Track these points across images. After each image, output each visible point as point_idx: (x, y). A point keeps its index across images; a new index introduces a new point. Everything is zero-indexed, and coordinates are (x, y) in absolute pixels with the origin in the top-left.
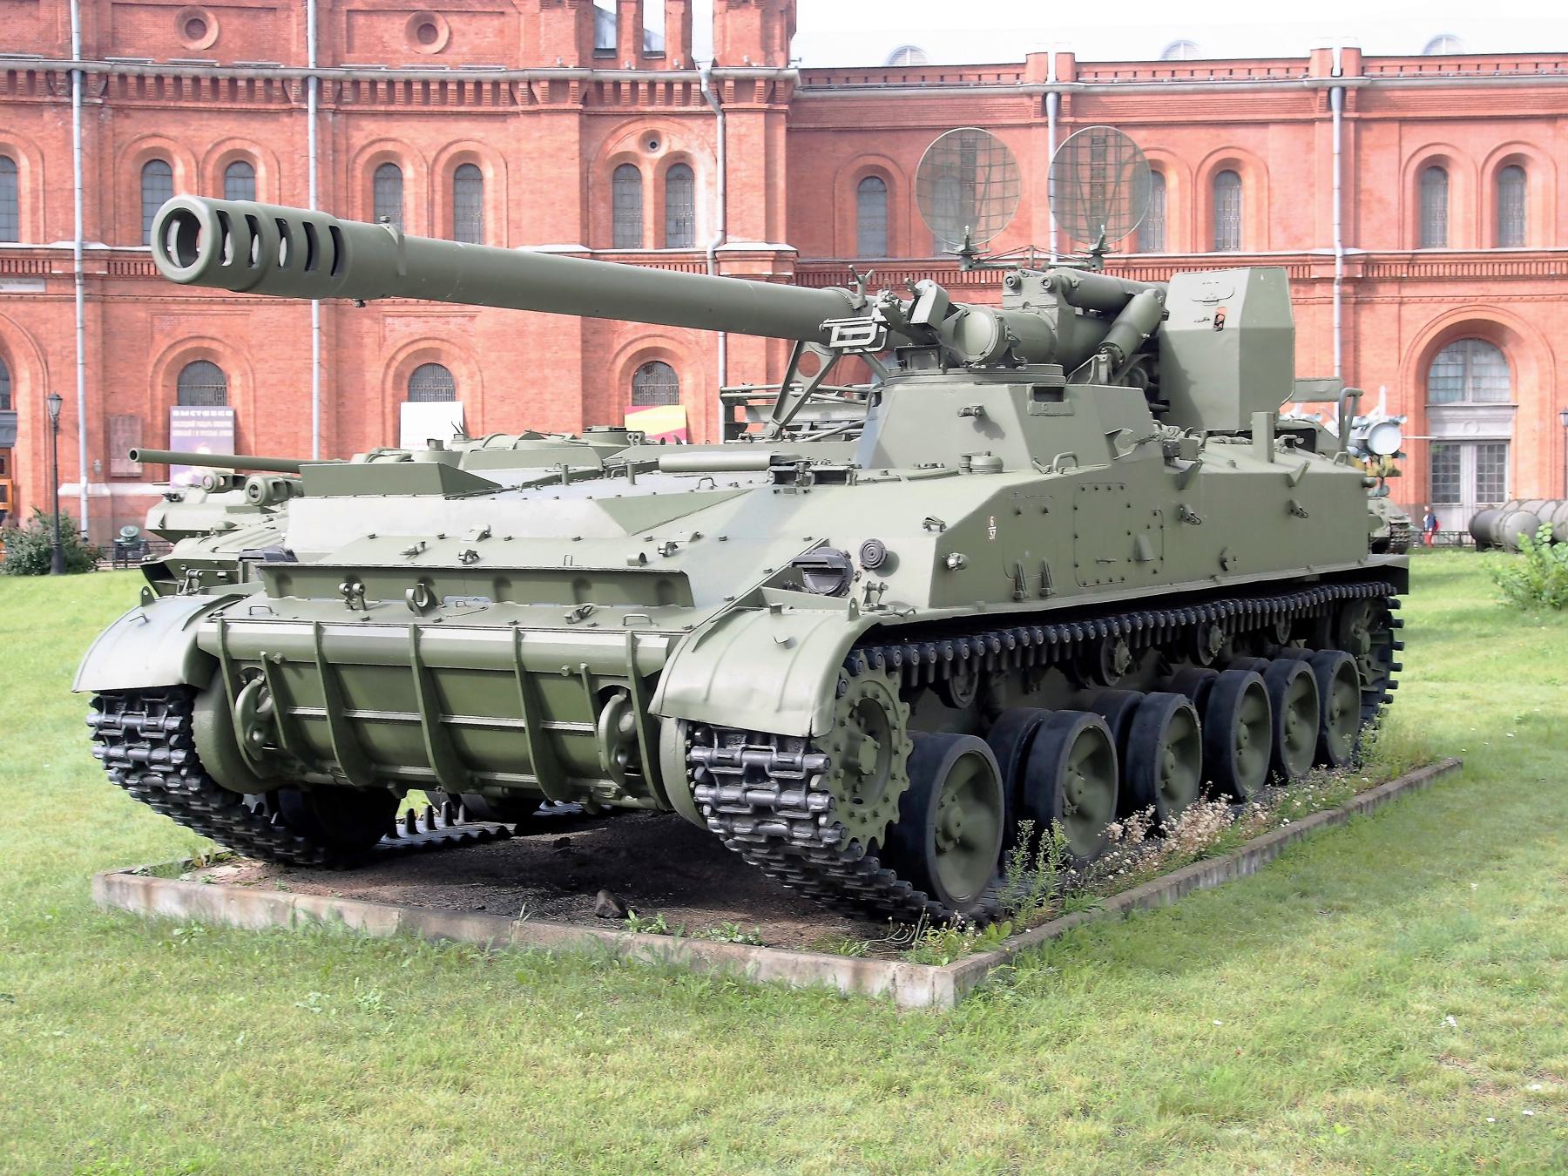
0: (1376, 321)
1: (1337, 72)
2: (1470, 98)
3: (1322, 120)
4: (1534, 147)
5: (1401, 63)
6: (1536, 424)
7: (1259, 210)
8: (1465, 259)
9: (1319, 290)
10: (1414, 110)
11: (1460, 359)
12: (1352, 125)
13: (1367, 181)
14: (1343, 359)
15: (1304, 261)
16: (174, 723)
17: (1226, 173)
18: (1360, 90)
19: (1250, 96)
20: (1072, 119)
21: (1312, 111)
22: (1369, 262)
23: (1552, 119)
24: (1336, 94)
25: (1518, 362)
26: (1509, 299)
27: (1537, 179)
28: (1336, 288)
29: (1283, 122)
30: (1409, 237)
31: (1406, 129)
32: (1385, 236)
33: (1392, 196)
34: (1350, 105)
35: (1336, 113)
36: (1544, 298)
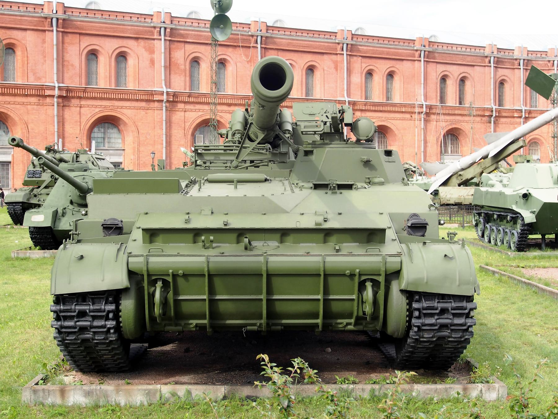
0: (71, 113)
1: (55, 12)
2: (106, 28)
3: (48, 30)
4: (130, 49)
5: (80, 11)
6: (132, 157)
7: (23, 65)
8: (105, 91)
9: (48, 100)
10: (85, 30)
11: (102, 130)
12: (61, 34)
13: (67, 57)
14: (58, 129)
15: (43, 88)
16: (112, 307)
18: (64, 20)
19: (19, 18)
21: (45, 27)
22: (68, 90)
23: (137, 39)
24: (54, 21)
25: (125, 132)
26: (122, 107)
27: (131, 61)
28: (55, 100)
29: (33, 30)
30: (83, 81)
31: (82, 37)
32: (74, 81)
33: (77, 64)
34: (60, 26)
35: (55, 28)
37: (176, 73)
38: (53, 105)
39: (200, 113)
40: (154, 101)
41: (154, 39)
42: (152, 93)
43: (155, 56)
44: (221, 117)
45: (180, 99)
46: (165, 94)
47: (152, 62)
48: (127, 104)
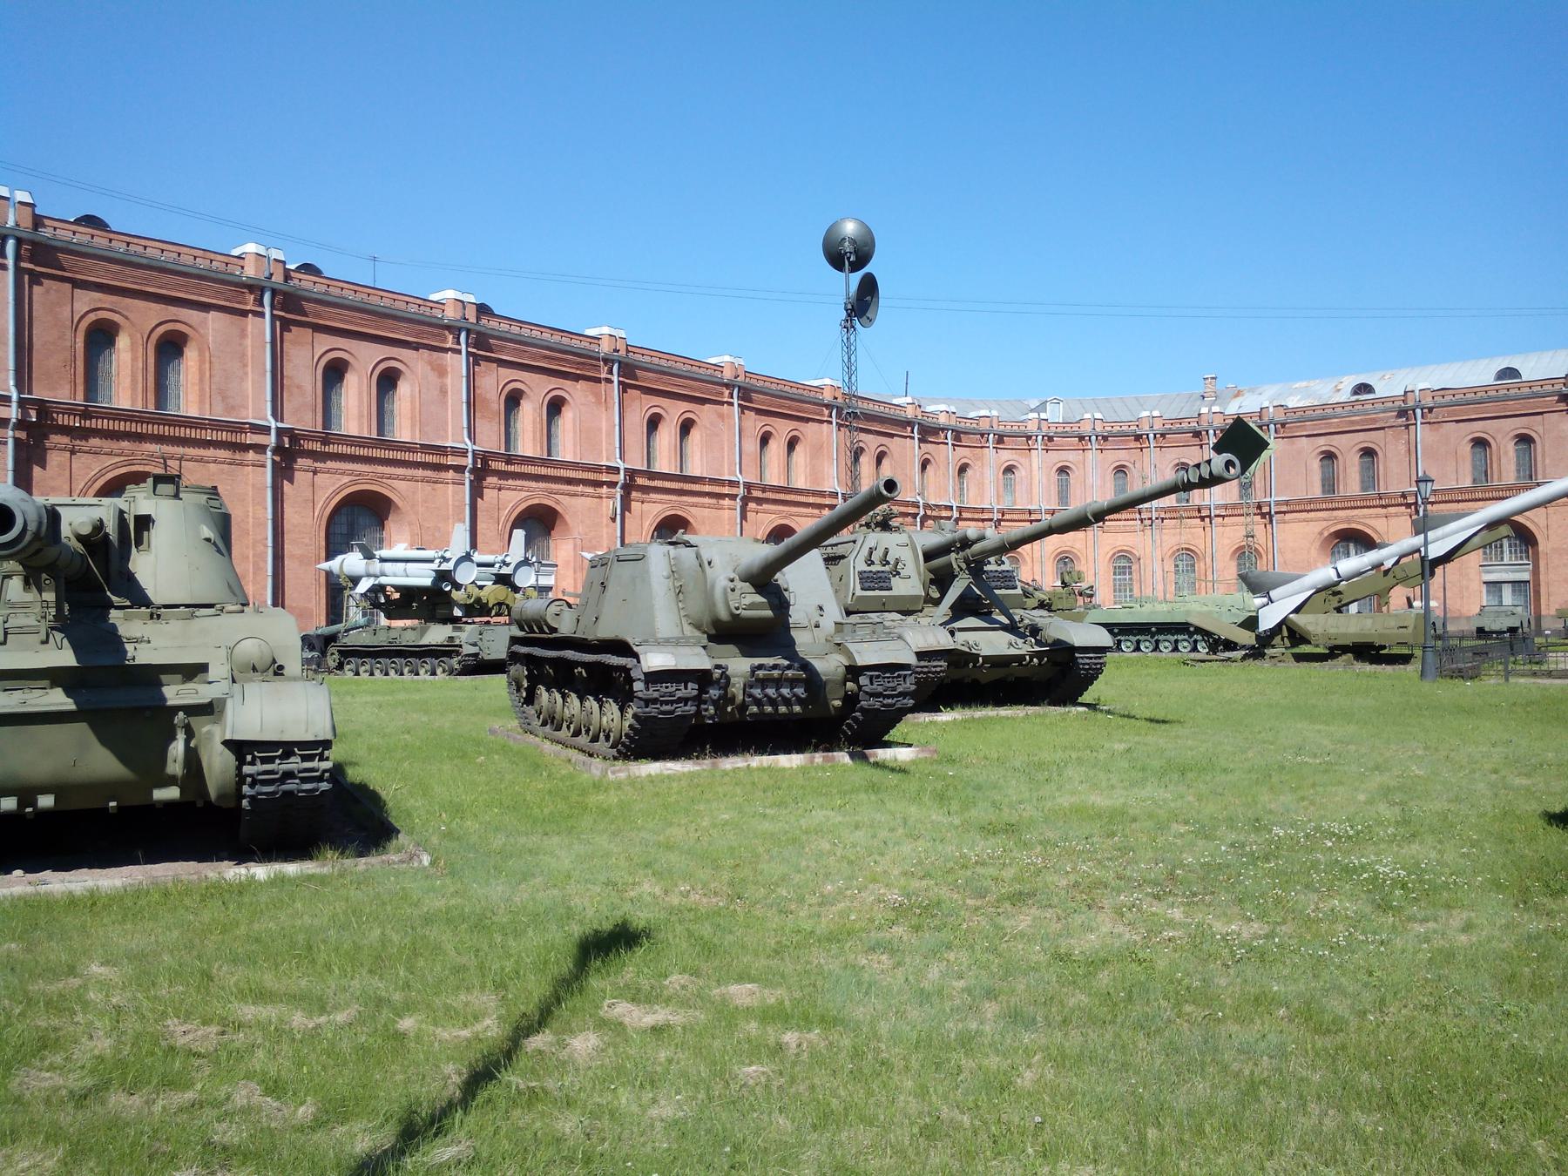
7: (201, 380)
9: (251, 455)
17: (170, 347)
20: (31, 266)
27: (404, 388)
28: (269, 453)
32: (300, 416)
33: (309, 388)
35: (267, 310)
36: (413, 479)
37: (483, 417)
38: (264, 466)
39: (524, 494)
40: (447, 468)
41: (446, 350)
42: (441, 450)
43: (449, 381)
44: (558, 502)
45: (494, 465)
46: (470, 455)
47: (443, 392)
48: (401, 471)
